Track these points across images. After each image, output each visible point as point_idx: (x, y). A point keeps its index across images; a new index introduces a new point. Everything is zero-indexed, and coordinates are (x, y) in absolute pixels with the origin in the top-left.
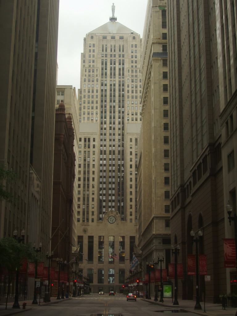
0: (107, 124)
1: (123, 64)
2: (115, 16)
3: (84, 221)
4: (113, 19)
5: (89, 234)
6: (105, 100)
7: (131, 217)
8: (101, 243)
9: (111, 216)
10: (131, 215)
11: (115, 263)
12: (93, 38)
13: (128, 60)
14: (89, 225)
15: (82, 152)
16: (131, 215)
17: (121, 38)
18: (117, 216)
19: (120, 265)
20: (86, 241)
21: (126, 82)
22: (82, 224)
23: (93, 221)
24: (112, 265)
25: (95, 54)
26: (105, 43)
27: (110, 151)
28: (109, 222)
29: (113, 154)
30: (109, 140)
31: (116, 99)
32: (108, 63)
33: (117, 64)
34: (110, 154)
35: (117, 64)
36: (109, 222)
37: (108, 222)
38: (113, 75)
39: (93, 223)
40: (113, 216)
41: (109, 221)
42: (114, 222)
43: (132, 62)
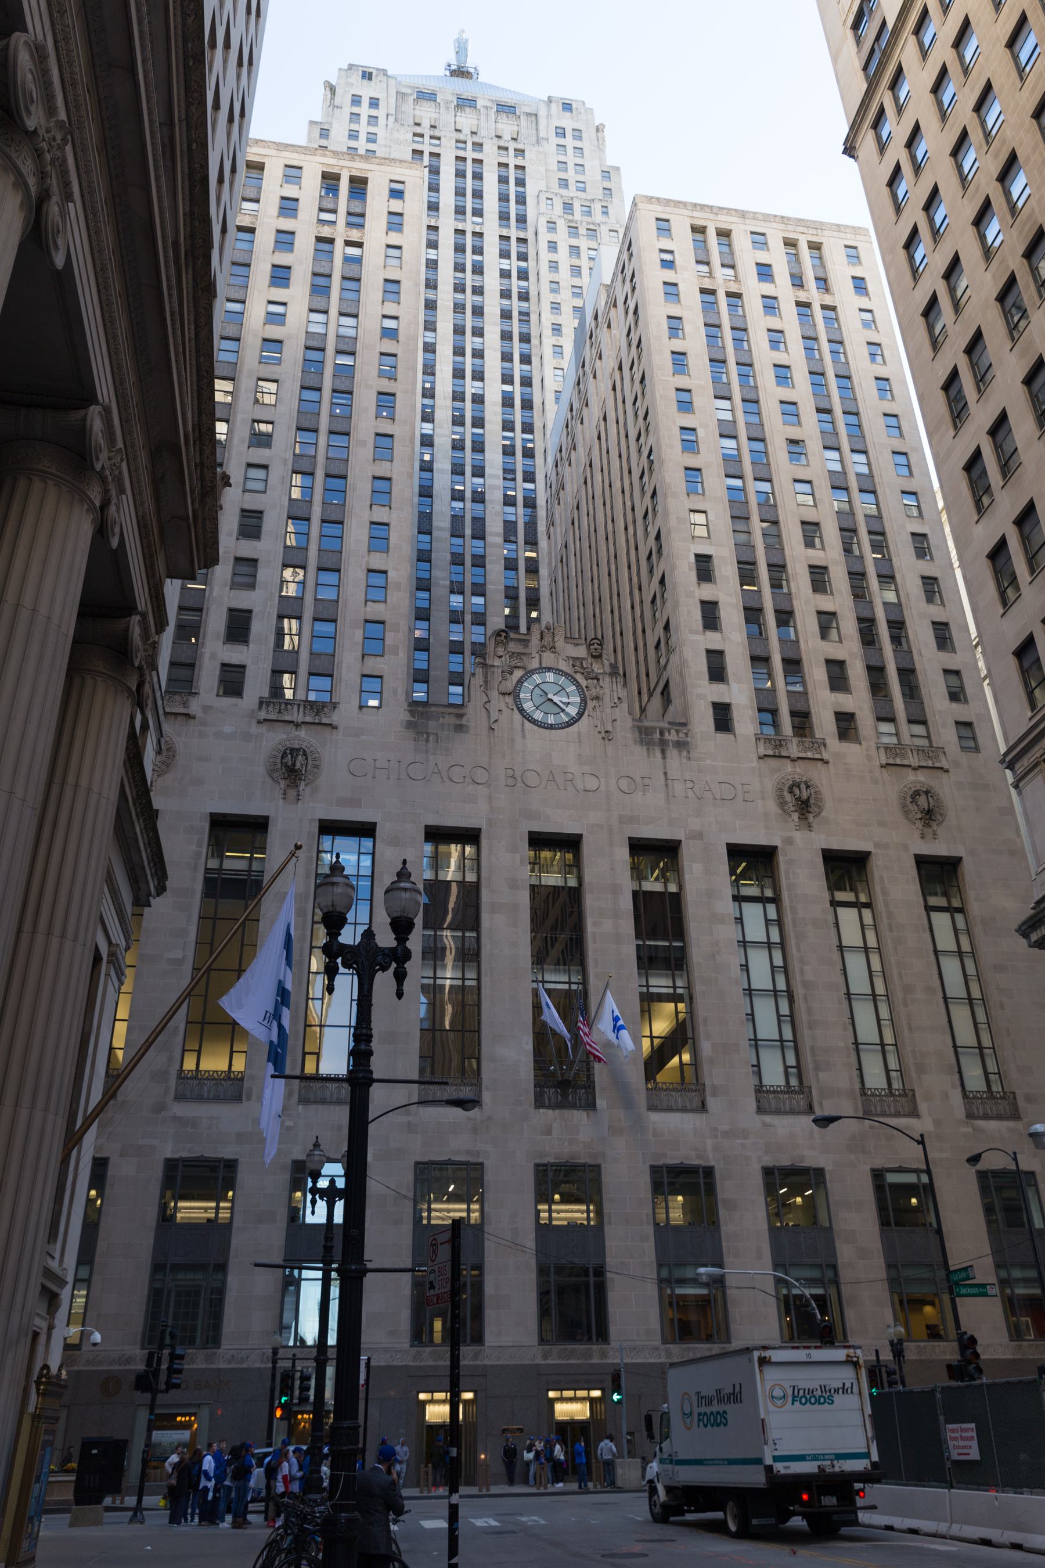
1: (521, 182)
2: (470, 64)
4: (460, 73)
7: (720, 687)
9: (543, 669)
10: (717, 672)
12: (370, 79)
13: (542, 169)
14: (332, 726)
16: (717, 672)
17: (506, 109)
18: (597, 668)
19: (655, 1117)
21: (543, 229)
22: (263, 715)
24: (579, 1116)
25: (380, 130)
26: (426, 113)
27: (457, 520)
29: (474, 537)
30: (449, 467)
32: (443, 169)
34: (456, 532)
36: (522, 711)
37: (517, 716)
40: (558, 672)
41: (528, 706)
42: (572, 722)
43: (564, 183)
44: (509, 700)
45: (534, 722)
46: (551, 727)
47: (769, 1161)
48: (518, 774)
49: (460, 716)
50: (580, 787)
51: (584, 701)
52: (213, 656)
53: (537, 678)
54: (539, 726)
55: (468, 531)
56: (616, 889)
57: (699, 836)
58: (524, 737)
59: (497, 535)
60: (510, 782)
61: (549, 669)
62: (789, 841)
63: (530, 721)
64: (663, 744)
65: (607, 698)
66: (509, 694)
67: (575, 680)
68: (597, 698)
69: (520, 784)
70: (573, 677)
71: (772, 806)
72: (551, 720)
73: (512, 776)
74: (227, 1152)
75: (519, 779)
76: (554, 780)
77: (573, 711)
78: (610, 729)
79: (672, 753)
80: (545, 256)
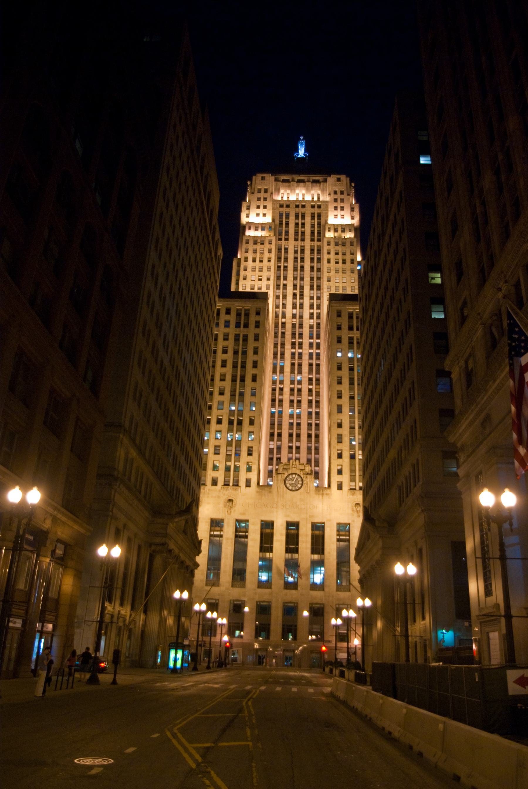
0: (287, 317)
3: (226, 484)
5: (237, 513)
6: (285, 275)
8: (266, 542)
11: (299, 588)
15: (232, 337)
20: (228, 532)
23: (248, 484)
28: (286, 486)
31: (305, 276)
33: (308, 219)
35: (308, 219)
37: (285, 488)
38: (300, 236)
39: (248, 488)
41: (288, 485)
45: (289, 489)
46: (293, 491)
47: (337, 602)
49: (271, 488)
52: (210, 475)
53: (290, 477)
55: (296, 372)
56: (307, 536)
57: (329, 520)
59: (306, 373)
61: (294, 474)
62: (353, 521)
64: (323, 494)
71: (350, 511)
72: (294, 489)
74: (217, 597)
77: (299, 486)
79: (325, 496)
80: (325, 257)
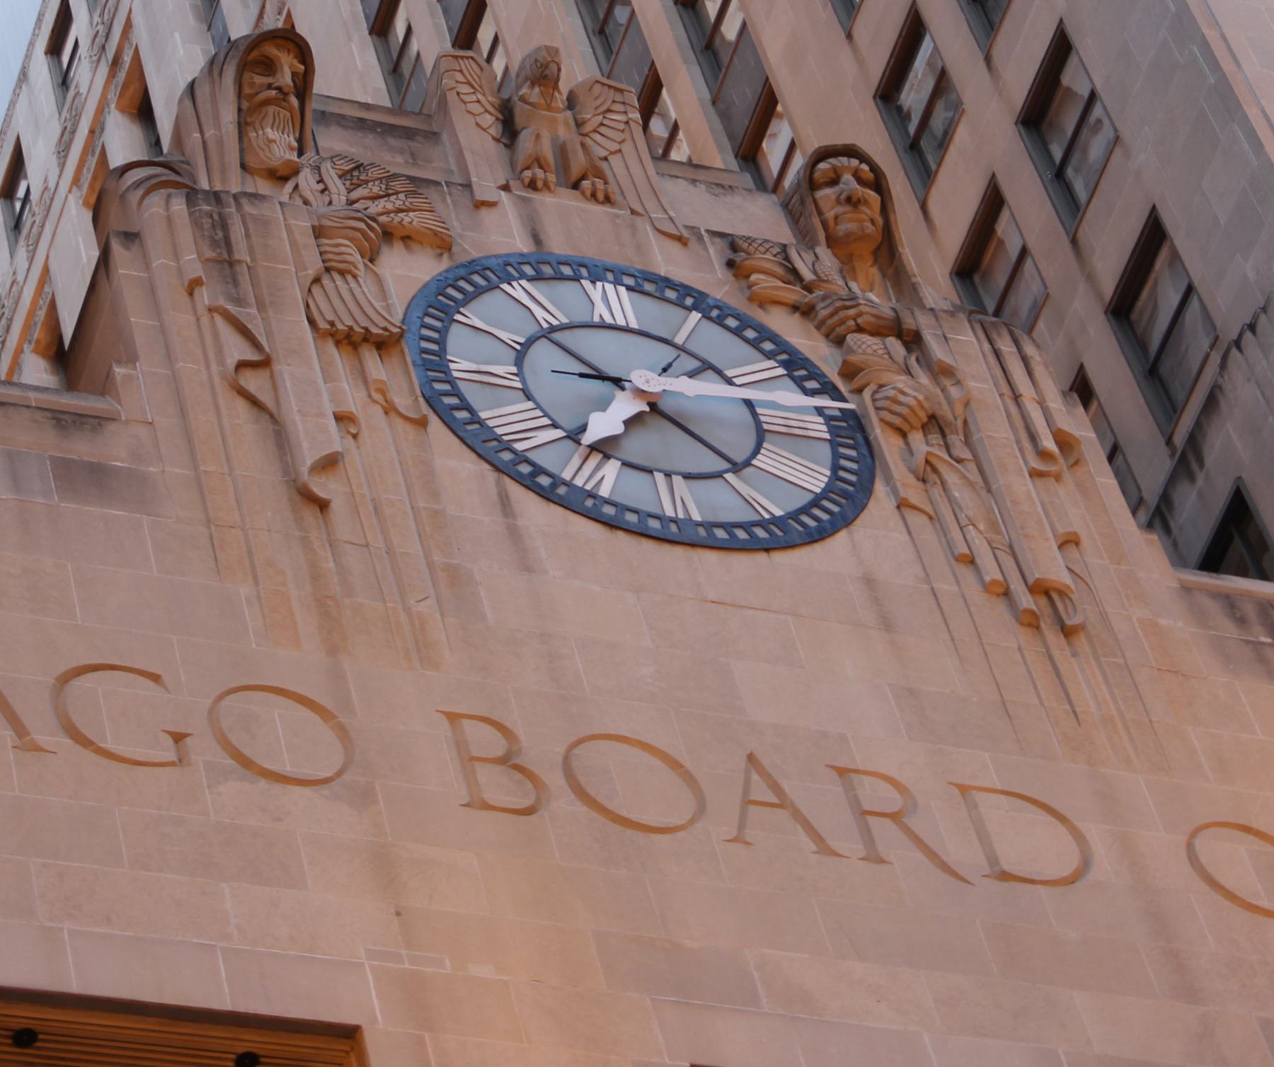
40: (648, 284)
44: (396, 378)
48: (543, 751)
50: (961, 850)
51: (849, 431)
54: (611, 524)
58: (526, 564)
60: (499, 786)
63: (547, 495)
65: (995, 430)
66: (384, 344)
67: (765, 334)
68: (934, 423)
69: (563, 803)
70: (746, 322)
73: (509, 761)
75: (555, 780)
76: (783, 802)
78: (1053, 567)
